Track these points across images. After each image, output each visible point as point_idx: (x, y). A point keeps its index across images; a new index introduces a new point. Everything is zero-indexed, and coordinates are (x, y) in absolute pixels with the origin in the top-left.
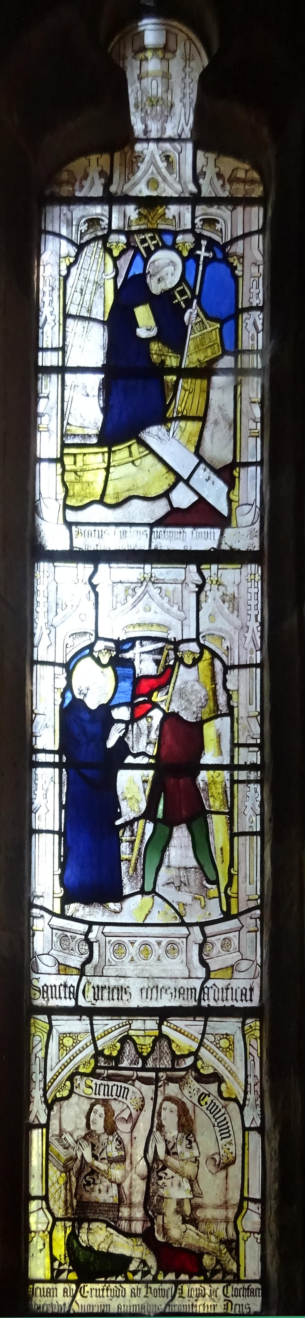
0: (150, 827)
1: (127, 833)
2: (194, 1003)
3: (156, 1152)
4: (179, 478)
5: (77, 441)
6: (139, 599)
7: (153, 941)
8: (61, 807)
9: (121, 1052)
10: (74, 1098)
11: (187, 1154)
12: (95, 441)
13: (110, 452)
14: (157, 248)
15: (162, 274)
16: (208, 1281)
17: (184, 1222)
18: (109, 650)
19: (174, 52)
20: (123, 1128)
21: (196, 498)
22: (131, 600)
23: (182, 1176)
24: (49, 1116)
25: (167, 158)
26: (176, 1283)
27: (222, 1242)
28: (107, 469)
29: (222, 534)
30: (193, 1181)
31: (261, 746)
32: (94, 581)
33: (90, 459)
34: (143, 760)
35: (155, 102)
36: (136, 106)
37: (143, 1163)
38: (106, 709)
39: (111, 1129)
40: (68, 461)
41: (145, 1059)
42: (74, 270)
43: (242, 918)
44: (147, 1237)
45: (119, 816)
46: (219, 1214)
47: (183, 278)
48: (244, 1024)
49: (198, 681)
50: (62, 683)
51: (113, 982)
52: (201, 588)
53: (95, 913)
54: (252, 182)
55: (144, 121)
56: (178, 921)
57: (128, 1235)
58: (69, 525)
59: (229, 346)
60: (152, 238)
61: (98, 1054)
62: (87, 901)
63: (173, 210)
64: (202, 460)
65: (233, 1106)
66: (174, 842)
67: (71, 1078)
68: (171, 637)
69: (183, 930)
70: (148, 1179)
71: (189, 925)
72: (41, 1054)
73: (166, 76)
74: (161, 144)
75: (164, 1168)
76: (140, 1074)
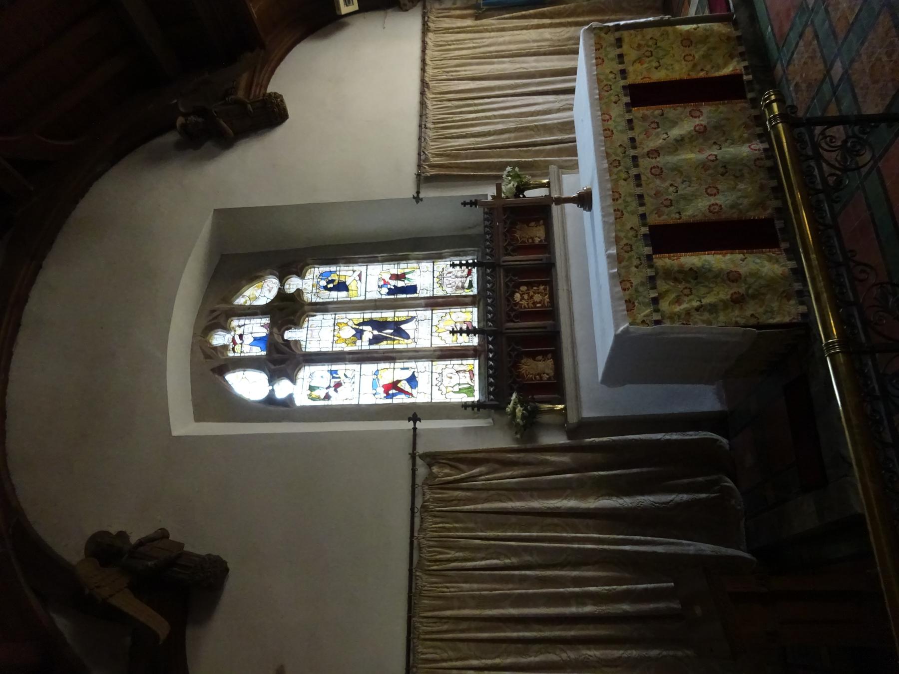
20: (451, 282)
38: (388, 289)
39: (451, 284)
44: (466, 277)
57: (466, 280)
63: (314, 283)
73: (293, 284)
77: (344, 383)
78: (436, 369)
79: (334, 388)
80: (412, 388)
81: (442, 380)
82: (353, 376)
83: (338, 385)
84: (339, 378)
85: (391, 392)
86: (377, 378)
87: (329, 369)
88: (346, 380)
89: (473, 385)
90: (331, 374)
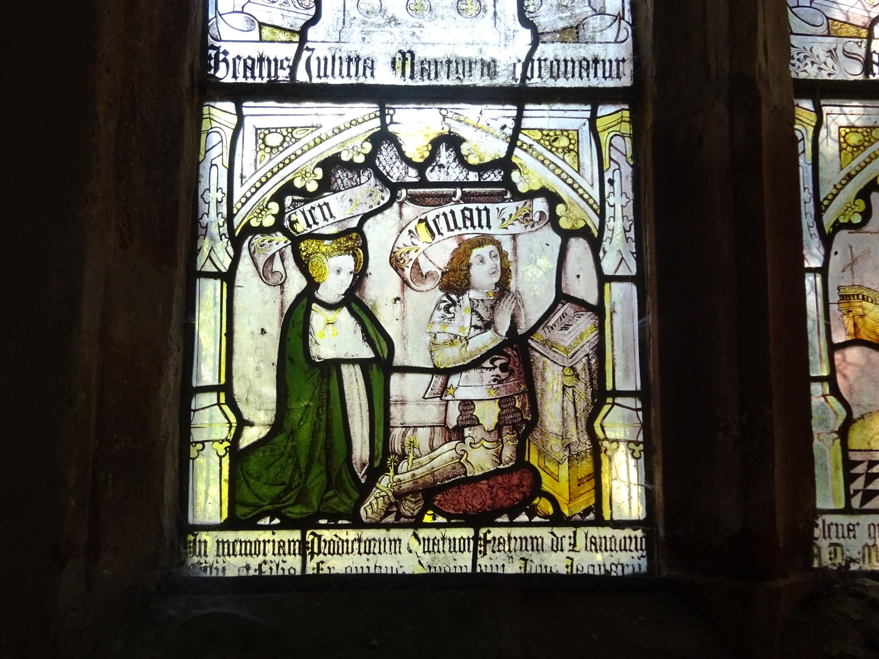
78: (550, 138)
89: (368, 511)
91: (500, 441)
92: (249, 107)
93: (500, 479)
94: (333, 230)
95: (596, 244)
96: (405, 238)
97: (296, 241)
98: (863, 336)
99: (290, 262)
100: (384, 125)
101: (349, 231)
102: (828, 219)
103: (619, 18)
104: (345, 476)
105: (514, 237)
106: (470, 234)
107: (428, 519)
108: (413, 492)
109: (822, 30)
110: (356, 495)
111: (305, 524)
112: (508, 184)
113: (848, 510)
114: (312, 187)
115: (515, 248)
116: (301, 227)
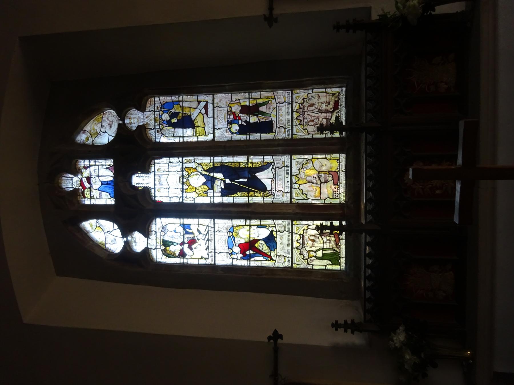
0: (260, 115)
1: (261, 120)
2: (290, 104)
3: (317, 111)
4: (200, 112)
5: (194, 133)
6: (220, 119)
7: (279, 114)
8: (256, 134)
9: (299, 119)
10: (307, 129)
11: (317, 105)
12: (194, 130)
13: (196, 126)
14: (162, 119)
15: (166, 117)
16: (340, 99)
17: (329, 105)
18: (229, 125)
19: (130, 117)
20: (313, 118)
21: (203, 109)
22: (221, 121)
23: (321, 105)
24: (311, 134)
25: (147, 117)
26: (340, 106)
27: (333, 97)
28: (199, 127)
29: (209, 103)
30: (322, 103)
31: (245, 93)
32: (217, 129)
33: (197, 131)
34: (248, 118)
35: (138, 120)
36: (139, 124)
37: (319, 114)
38: (239, 125)
39: (313, 121)
40: (198, 135)
41: (300, 114)
42: (166, 135)
43: (275, 95)
44: (332, 112)
45: (258, 122)
46: (328, 97)
47: (167, 113)
48: (294, 94)
49: (234, 107)
50: (235, 134)
51: (287, 122)
52: (218, 107)
53: (275, 125)
54: (151, 100)
55: (141, 123)
56: (276, 109)
57: (332, 116)
58: (208, 134)
59: (178, 103)
60: (160, 120)
61: (300, 124)
62: (272, 128)
63: (156, 116)
64: (197, 108)
65: (309, 95)
66: (262, 110)
67: (304, 130)
68: (227, 113)
69: (277, 107)
70: (322, 113)
71: (276, 106)
72: (300, 136)
73: (134, 118)
74: (145, 119)
75: (320, 109)
76: (303, 115)
77: (198, 239)
78: (297, 230)
79: (188, 245)
80: (270, 250)
81: (303, 243)
82: (206, 232)
83: (192, 242)
84: (192, 233)
85: (248, 253)
86: (232, 235)
87: (182, 223)
88: (200, 237)
89: (338, 251)
90: (184, 229)
91: (331, 237)
92: (294, 263)
93: (335, 237)
94: (308, 254)
95: (309, 225)
96: (309, 246)
97: (309, 258)
98: (319, 195)
99: (311, 259)
100: (296, 248)
101: (308, 252)
102: (306, 199)
103: (283, 221)
104: (335, 253)
105: (308, 234)
106: (308, 239)
107: (339, 245)
108: (337, 246)
109: (284, 198)
110: (337, 252)
111: (340, 257)
112: (302, 235)
113: (339, 199)
114: (303, 256)
115: (310, 234)
116: (307, 257)
